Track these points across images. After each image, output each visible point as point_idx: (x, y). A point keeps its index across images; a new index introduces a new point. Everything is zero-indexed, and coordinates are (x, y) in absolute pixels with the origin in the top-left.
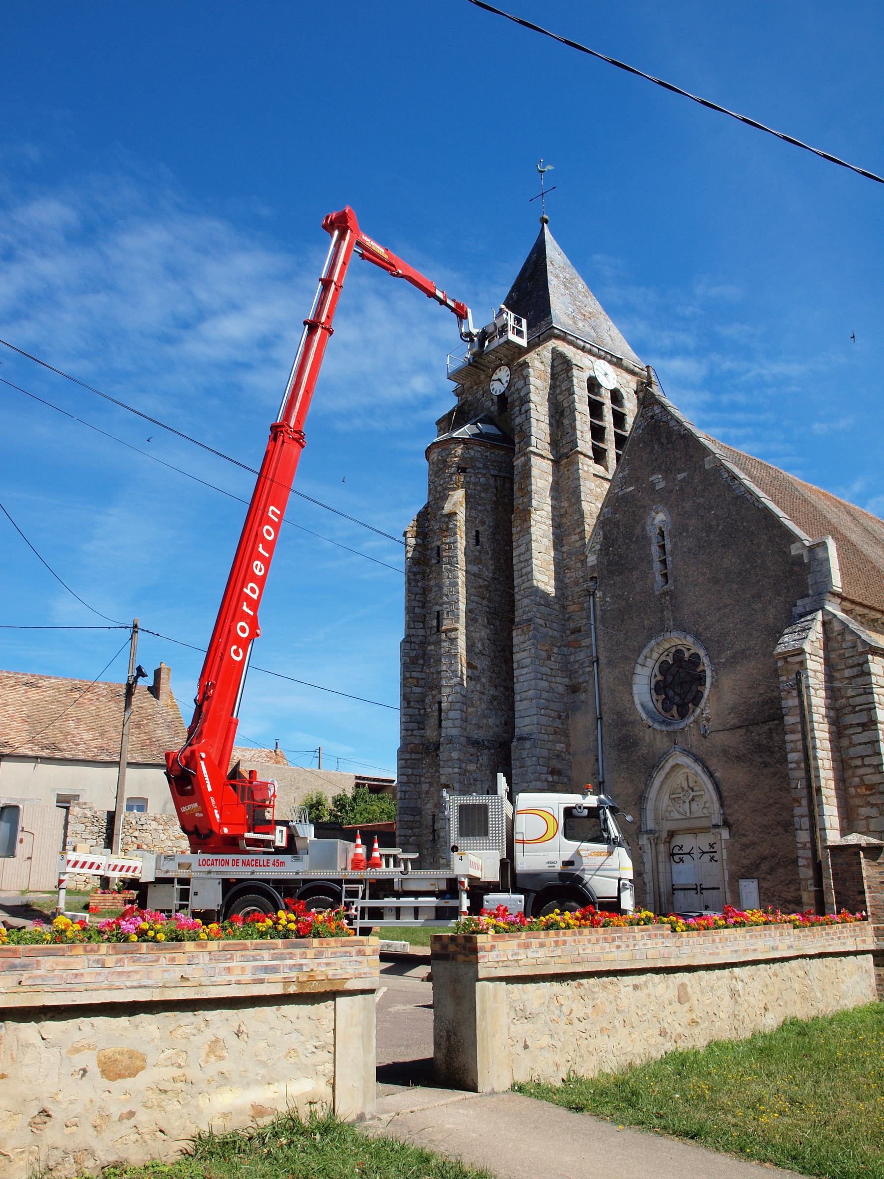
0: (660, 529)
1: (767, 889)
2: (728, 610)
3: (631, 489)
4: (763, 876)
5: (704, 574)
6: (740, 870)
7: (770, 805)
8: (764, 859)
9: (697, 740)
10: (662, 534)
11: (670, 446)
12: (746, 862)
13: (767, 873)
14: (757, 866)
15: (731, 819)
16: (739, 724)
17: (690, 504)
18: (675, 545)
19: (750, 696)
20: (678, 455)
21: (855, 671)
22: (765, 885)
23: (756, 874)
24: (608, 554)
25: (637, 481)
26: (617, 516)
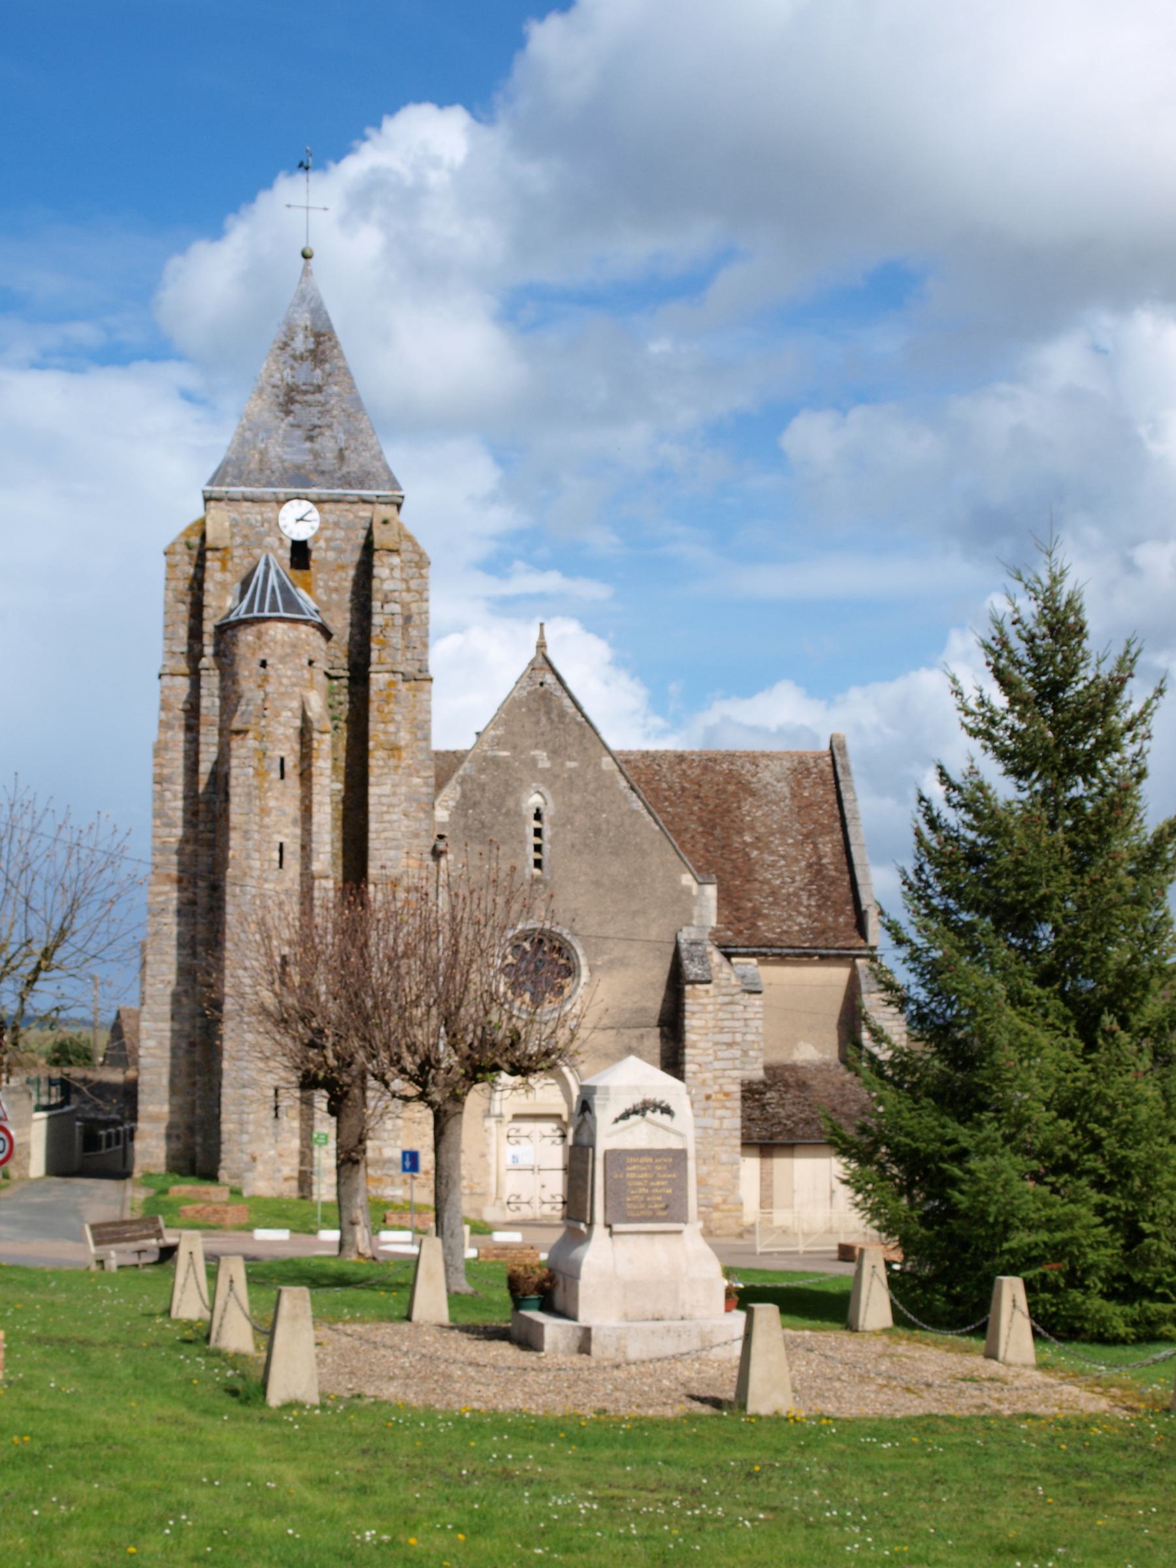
0: (538, 810)
10: (538, 816)
11: (561, 726)
18: (555, 835)
20: (570, 740)
21: (727, 999)
24: (466, 816)
25: (515, 748)
26: (483, 777)
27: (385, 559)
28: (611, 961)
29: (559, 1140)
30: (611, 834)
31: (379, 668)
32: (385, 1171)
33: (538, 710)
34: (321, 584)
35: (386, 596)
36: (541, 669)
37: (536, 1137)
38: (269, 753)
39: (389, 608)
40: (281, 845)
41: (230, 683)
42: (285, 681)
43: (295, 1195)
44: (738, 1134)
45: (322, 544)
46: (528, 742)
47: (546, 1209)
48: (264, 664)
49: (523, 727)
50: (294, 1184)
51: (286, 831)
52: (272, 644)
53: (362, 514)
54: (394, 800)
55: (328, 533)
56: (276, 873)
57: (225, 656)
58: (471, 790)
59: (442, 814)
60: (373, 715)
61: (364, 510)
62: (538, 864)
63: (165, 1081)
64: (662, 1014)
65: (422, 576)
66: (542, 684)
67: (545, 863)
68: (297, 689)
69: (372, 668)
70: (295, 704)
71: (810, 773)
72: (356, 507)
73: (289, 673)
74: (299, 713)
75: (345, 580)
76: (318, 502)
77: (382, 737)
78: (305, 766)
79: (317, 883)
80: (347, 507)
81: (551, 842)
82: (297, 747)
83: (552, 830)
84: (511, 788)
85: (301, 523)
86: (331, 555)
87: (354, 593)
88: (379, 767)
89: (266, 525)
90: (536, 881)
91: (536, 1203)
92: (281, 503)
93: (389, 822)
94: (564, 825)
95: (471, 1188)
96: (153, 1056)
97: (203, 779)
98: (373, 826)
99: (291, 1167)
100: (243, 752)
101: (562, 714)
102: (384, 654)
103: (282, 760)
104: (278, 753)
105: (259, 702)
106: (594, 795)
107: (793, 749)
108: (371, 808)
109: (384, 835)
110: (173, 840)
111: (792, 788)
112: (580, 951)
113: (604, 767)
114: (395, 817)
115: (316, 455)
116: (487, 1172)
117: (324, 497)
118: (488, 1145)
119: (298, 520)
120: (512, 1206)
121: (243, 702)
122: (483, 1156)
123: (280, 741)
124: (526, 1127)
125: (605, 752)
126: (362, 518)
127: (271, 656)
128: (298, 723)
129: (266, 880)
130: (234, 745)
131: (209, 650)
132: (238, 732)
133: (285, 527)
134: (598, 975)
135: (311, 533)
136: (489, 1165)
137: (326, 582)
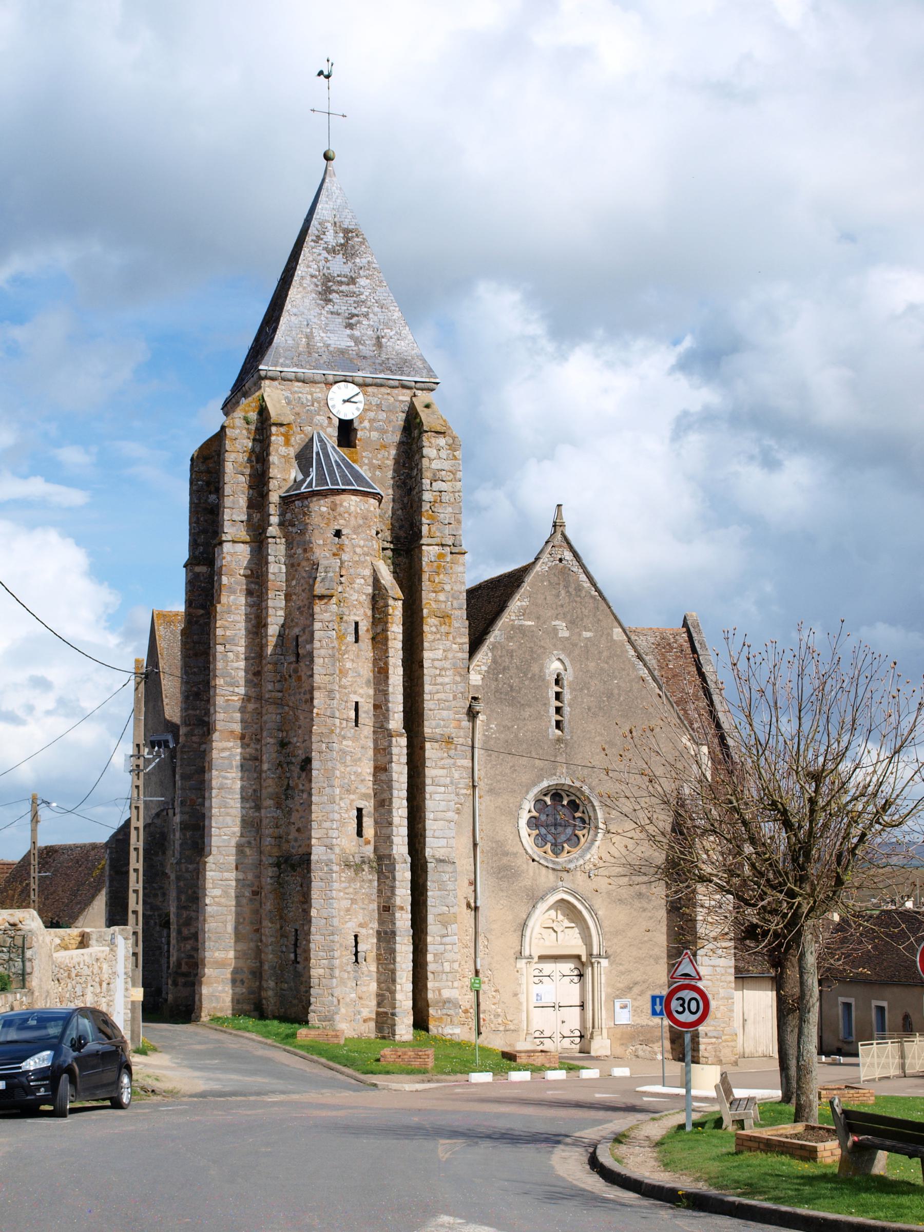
0: (558, 676)
1: (637, 1007)
3: (530, 623)
4: (634, 997)
5: (601, 735)
7: (646, 942)
9: (583, 881)
10: (557, 682)
11: (578, 599)
12: (621, 985)
13: (638, 995)
14: (630, 988)
15: (610, 952)
16: (623, 873)
17: (593, 664)
18: (574, 699)
22: (636, 1004)
23: (628, 996)
24: (497, 680)
25: (538, 618)
26: (511, 644)
27: (433, 440)
29: (576, 979)
30: (622, 699)
31: (430, 541)
32: (445, 1011)
33: (559, 584)
34: (366, 461)
35: (434, 475)
36: (561, 546)
37: (556, 976)
38: (345, 618)
39: (438, 485)
40: (357, 703)
41: (300, 551)
42: (358, 550)
43: (373, 1036)
44: (733, 970)
45: (366, 424)
46: (549, 613)
47: (566, 1043)
48: (338, 534)
49: (545, 599)
50: (372, 1025)
51: (361, 691)
52: (346, 515)
53: (401, 398)
54: (447, 664)
55: (371, 415)
56: (353, 731)
57: (294, 525)
58: (501, 657)
59: (475, 678)
60: (426, 585)
61: (403, 395)
62: (558, 725)
63: (230, 928)
65: (455, 458)
66: (561, 560)
67: (566, 724)
68: (368, 558)
69: (424, 541)
70: (368, 572)
71: (672, 648)
72: (396, 391)
73: (362, 543)
74: (370, 581)
75: (388, 459)
76: (362, 385)
77: (434, 605)
78: (379, 630)
79: (394, 740)
80: (389, 391)
81: (570, 705)
82: (370, 613)
83: (571, 693)
84: (535, 656)
85: (347, 404)
86: (375, 435)
87: (395, 471)
88: (432, 633)
89: (316, 404)
90: (559, 740)
91: (557, 1038)
92: (329, 384)
93: (441, 684)
94: (581, 690)
95: (505, 1025)
96: (219, 904)
97: (272, 641)
98: (427, 688)
99: (369, 1009)
100: (327, 616)
101: (579, 588)
102: (433, 528)
103: (357, 624)
104: (353, 618)
105: (338, 569)
106: (607, 663)
107: (654, 627)
108: (425, 671)
109: (436, 697)
110: (236, 698)
111: (659, 661)
113: (615, 637)
114: (447, 680)
115: (357, 341)
116: (519, 1009)
117: (369, 381)
119: (345, 401)
121: (321, 569)
122: (516, 995)
123: (354, 606)
124: (548, 967)
125: (616, 624)
126: (403, 401)
127: (346, 526)
128: (370, 590)
129: (344, 738)
130: (317, 609)
131: (274, 520)
132: (322, 597)
133: (334, 406)
135: (357, 413)
136: (521, 1003)
137: (370, 459)
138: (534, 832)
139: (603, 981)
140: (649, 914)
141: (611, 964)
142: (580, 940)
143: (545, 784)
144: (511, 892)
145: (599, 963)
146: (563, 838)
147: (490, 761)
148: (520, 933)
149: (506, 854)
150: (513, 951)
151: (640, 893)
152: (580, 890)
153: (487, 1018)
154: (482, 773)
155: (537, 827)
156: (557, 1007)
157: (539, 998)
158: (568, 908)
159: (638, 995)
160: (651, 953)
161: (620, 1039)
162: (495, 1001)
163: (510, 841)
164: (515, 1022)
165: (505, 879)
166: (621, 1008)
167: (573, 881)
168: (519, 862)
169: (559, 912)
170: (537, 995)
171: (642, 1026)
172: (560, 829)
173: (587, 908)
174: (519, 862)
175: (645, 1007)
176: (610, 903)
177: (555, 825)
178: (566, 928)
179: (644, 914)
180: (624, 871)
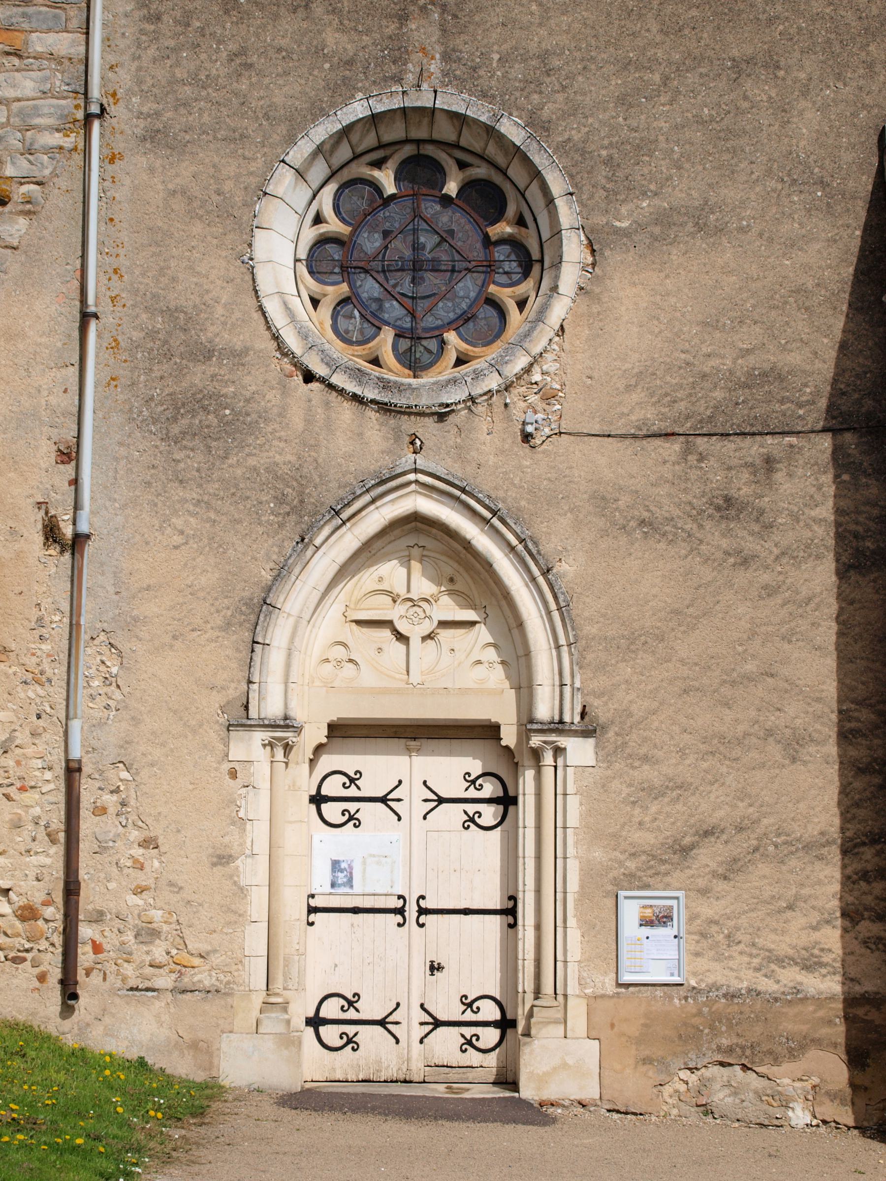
1: (712, 922)
2: (657, 78)
4: (701, 883)
6: (621, 863)
7: (748, 678)
8: (707, 833)
9: (501, 452)
12: (647, 839)
14: (685, 851)
15: (601, 711)
19: (706, 349)
22: (708, 909)
23: (677, 876)
28: (663, 219)
29: (489, 814)
64: (837, 393)
112: (557, 184)
118: (241, 823)
120: (330, 1034)
122: (223, 859)
134: (612, 257)
136: (242, 892)
138: (330, 289)
139: (573, 820)
140: (766, 577)
141: (605, 756)
142: (499, 672)
143: (357, 110)
144: (212, 488)
145: (558, 751)
146: (445, 311)
147: (156, 37)
148: (247, 636)
149: (207, 354)
150: (217, 699)
151: (728, 499)
152: (485, 484)
153: (110, 941)
154: (124, 78)
155: (346, 271)
156: (412, 911)
157: (341, 877)
158: (454, 556)
159: (714, 874)
160: (772, 719)
161: (639, 1041)
162: (142, 879)
163: (220, 311)
164: (215, 959)
165: (197, 441)
166: (647, 923)
167: (460, 453)
168: (251, 382)
169: (416, 566)
170: (336, 865)
171: (731, 996)
172: (432, 281)
173: (512, 549)
174: (251, 382)
175: (743, 921)
176: (604, 533)
177: (416, 267)
178: (443, 624)
179: (741, 577)
180: (664, 419)
